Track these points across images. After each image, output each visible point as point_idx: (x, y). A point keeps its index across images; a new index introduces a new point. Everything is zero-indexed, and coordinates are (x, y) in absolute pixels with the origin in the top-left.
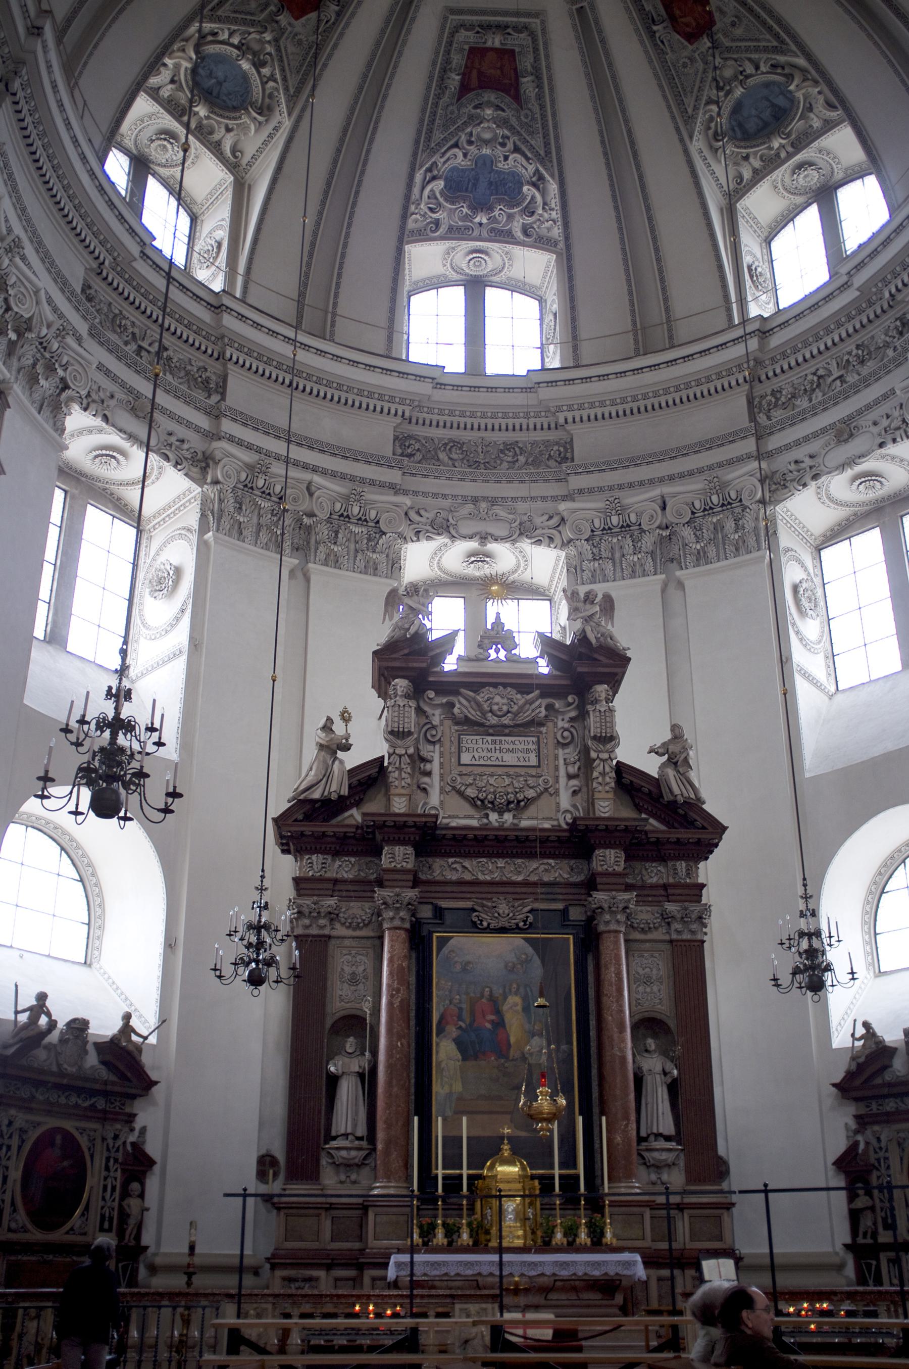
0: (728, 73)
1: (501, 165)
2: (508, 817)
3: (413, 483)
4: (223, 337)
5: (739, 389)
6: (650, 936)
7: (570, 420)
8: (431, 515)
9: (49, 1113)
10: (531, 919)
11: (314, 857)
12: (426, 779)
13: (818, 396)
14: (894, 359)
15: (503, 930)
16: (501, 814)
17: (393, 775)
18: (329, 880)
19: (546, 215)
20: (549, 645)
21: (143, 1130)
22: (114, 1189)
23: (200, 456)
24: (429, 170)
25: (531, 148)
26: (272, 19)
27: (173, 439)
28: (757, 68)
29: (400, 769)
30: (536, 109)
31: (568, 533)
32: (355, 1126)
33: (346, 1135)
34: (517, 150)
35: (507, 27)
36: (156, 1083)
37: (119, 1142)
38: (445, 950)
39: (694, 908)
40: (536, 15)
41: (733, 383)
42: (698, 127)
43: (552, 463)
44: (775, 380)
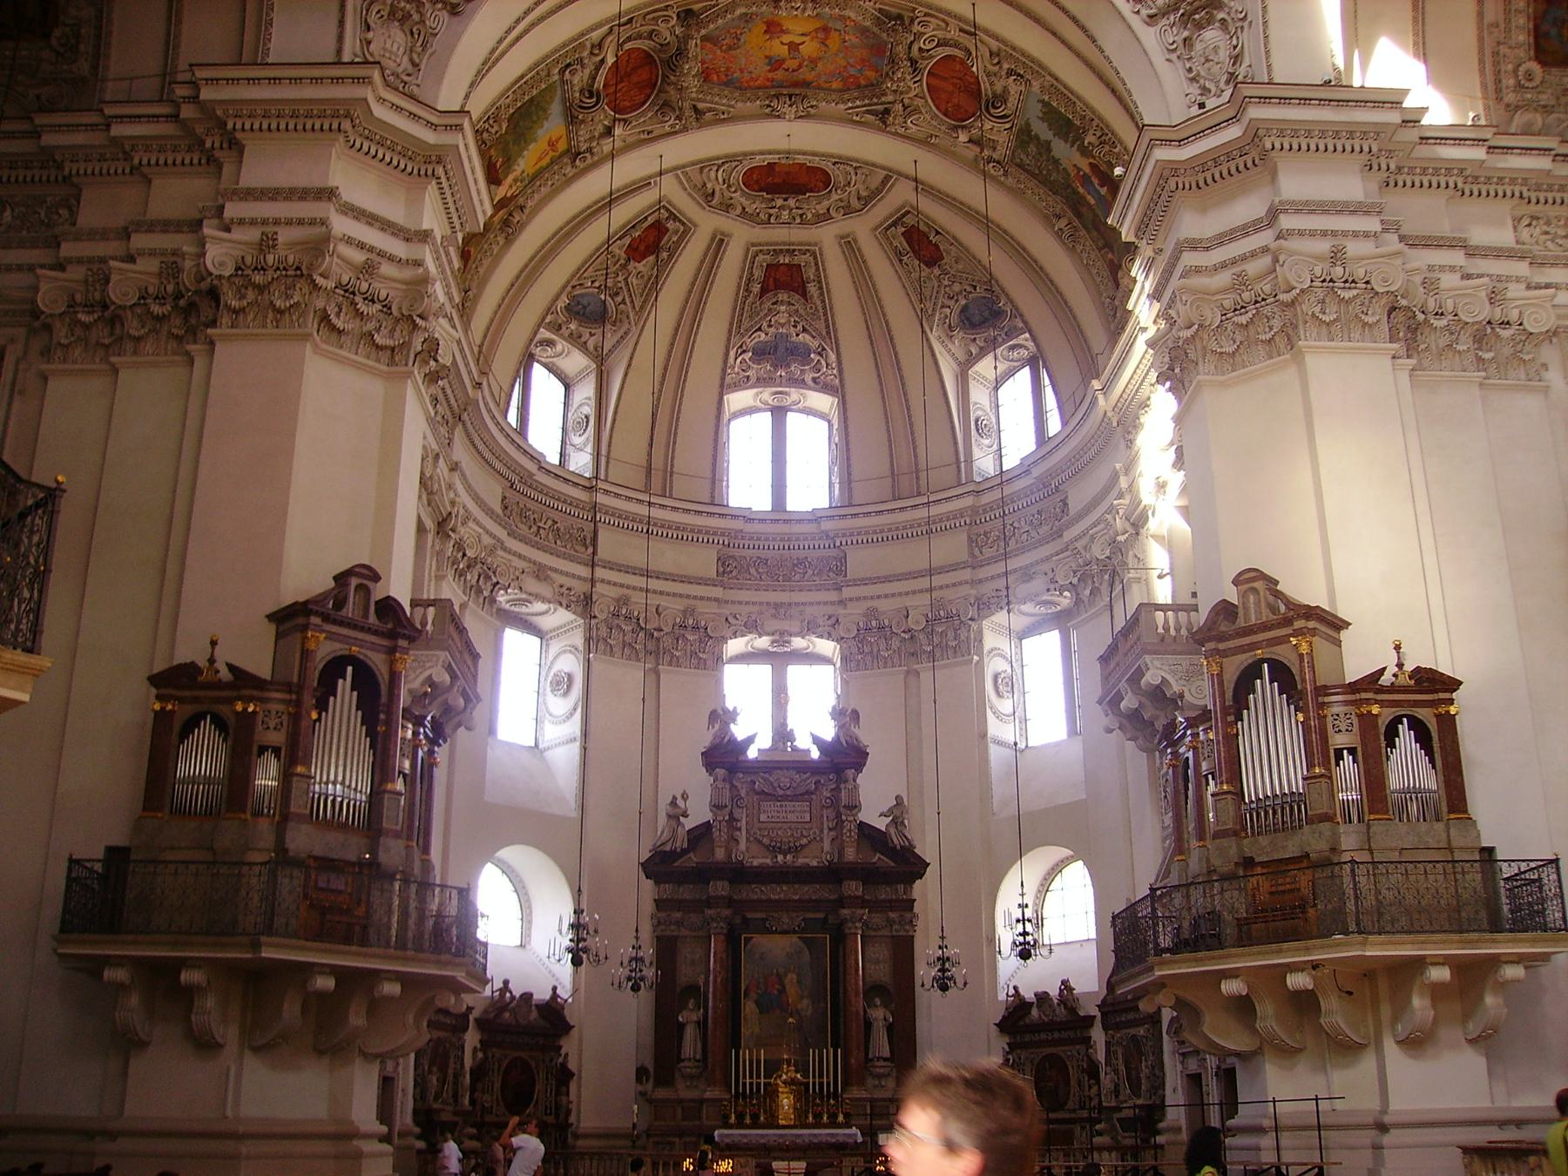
1: (794, 338)
6: (880, 933)
12: (738, 833)
20: (817, 740)
21: (567, 1055)
24: (741, 346)
25: (816, 330)
27: (564, 590)
28: (975, 288)
30: (819, 302)
32: (695, 1053)
34: (804, 330)
36: (573, 1027)
37: (554, 1063)
38: (749, 947)
39: (908, 915)
40: (816, 245)
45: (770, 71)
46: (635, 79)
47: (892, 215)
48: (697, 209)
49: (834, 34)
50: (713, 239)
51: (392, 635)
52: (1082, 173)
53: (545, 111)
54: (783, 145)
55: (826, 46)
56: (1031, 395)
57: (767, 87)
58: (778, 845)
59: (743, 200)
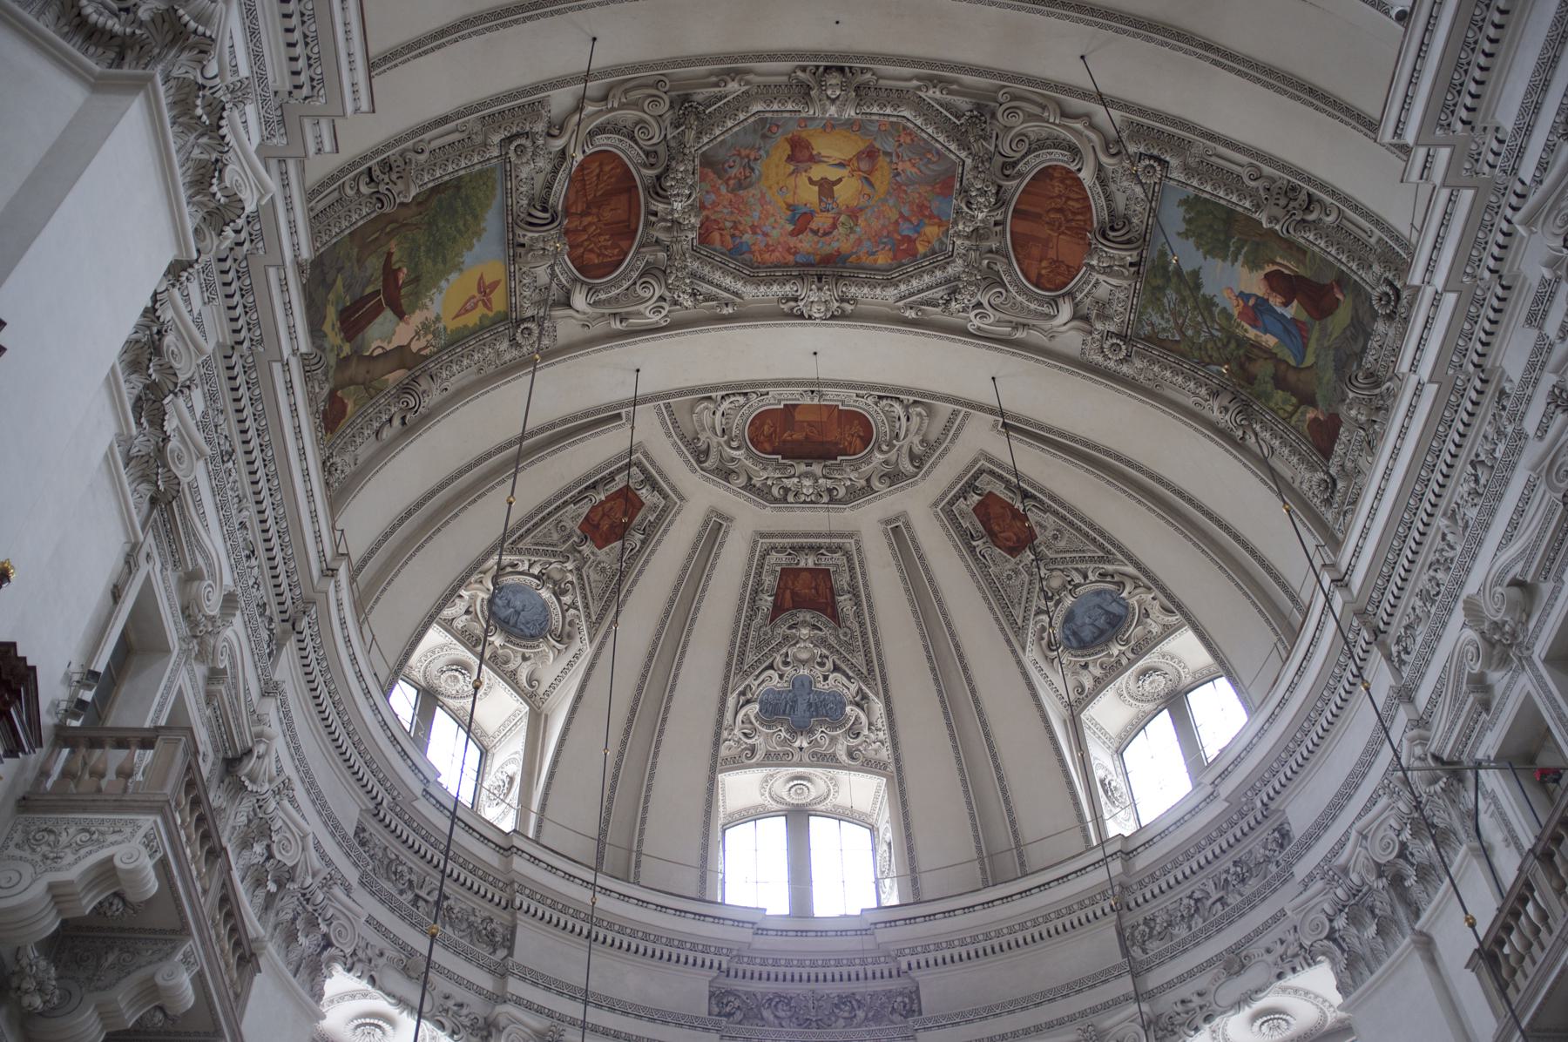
0: (1056, 583)
1: (821, 686)
5: (1107, 920)
7: (914, 965)
13: (1198, 923)
14: (1278, 876)
19: (873, 736)
24: (743, 693)
25: (853, 666)
26: (574, 549)
28: (1085, 577)
30: (855, 626)
34: (836, 669)
35: (820, 548)
40: (851, 536)
41: (1099, 913)
42: (1030, 638)
43: (896, 1018)
44: (1146, 907)
45: (794, 234)
46: (607, 215)
47: (960, 478)
48: (686, 469)
49: (882, 161)
50: (706, 523)
52: (1251, 302)
53: (476, 217)
54: (807, 370)
55: (871, 184)
56: (1176, 746)
57: (786, 265)
59: (749, 463)
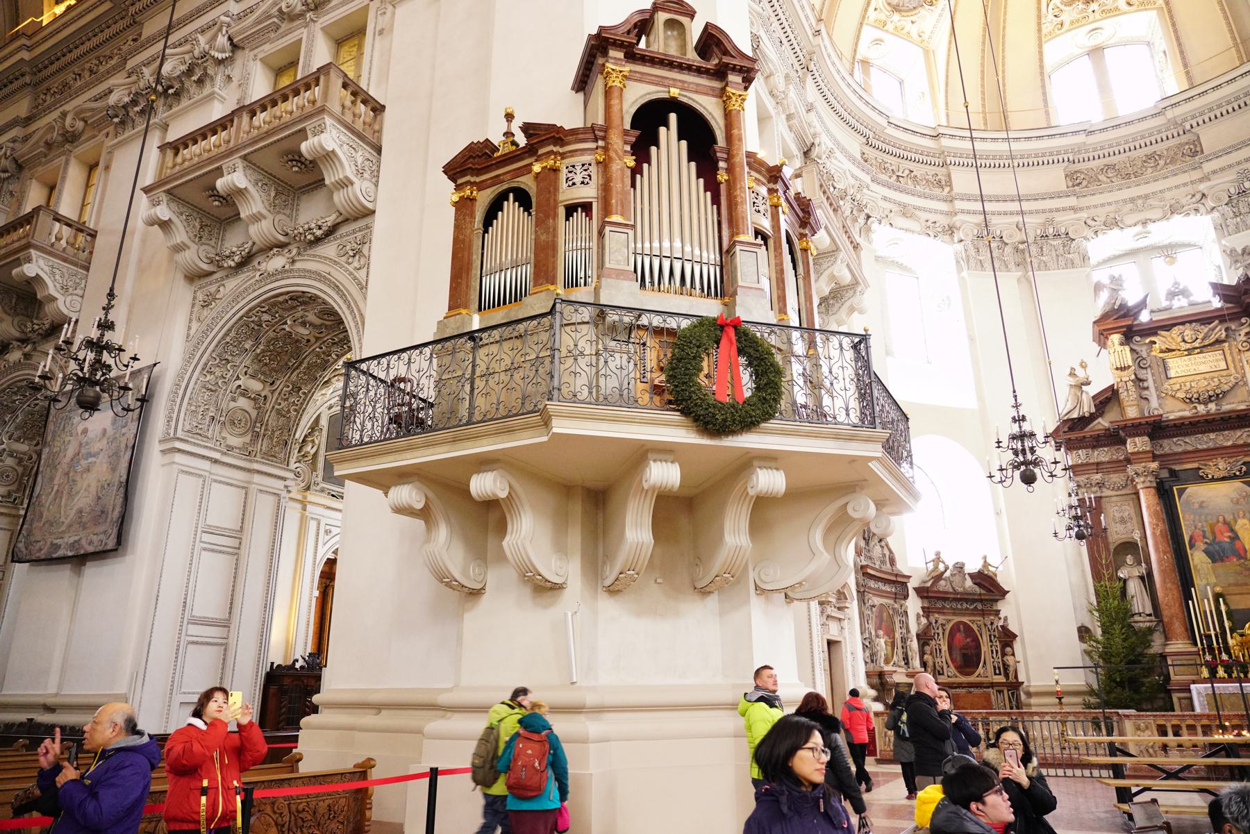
2: (1212, 407)
3: (1084, 202)
4: (943, 152)
7: (1195, 124)
8: (1103, 219)
9: (954, 614)
10: (1244, 469)
11: (1080, 452)
15: (1224, 479)
16: (1206, 404)
17: (1123, 395)
18: (1093, 464)
20: (1220, 289)
21: (1006, 619)
22: (997, 652)
23: (947, 228)
29: (1127, 390)
31: (1210, 203)
32: (1144, 607)
33: (1140, 614)
36: (1008, 592)
37: (994, 626)
38: (1184, 496)
51: (720, 73)
58: (1196, 396)
